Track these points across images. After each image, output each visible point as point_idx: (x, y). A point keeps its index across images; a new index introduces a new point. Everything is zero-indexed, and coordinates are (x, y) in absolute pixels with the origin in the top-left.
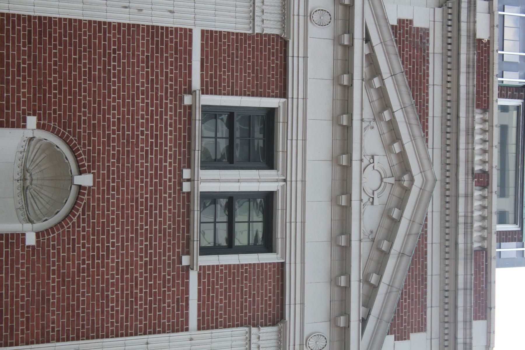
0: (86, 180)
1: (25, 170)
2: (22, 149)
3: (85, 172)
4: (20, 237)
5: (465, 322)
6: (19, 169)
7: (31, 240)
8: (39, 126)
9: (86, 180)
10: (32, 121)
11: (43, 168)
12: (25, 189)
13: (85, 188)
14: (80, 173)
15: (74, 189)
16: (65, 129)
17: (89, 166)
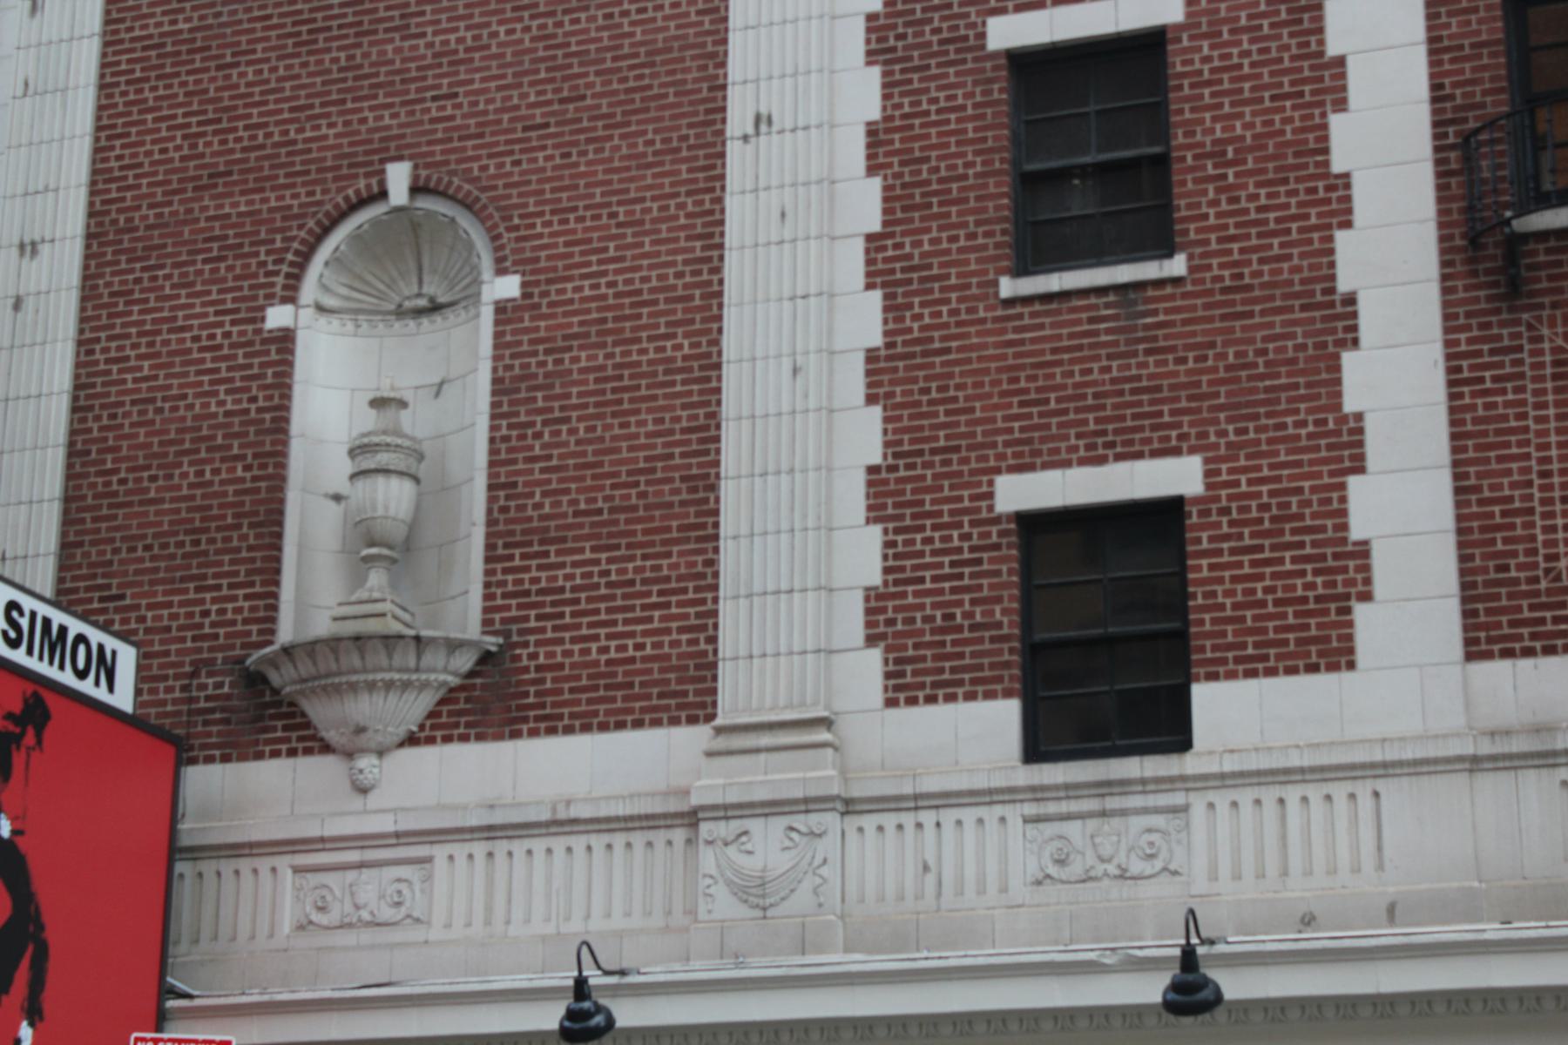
0: (398, 177)
1: (400, 313)
2: (350, 326)
3: (382, 184)
4: (501, 308)
6: (397, 325)
7: (509, 287)
8: (290, 298)
9: (398, 177)
10: (277, 317)
11: (395, 274)
12: (435, 308)
13: (415, 177)
14: (383, 194)
15: (426, 203)
16: (293, 239)
17: (367, 175)
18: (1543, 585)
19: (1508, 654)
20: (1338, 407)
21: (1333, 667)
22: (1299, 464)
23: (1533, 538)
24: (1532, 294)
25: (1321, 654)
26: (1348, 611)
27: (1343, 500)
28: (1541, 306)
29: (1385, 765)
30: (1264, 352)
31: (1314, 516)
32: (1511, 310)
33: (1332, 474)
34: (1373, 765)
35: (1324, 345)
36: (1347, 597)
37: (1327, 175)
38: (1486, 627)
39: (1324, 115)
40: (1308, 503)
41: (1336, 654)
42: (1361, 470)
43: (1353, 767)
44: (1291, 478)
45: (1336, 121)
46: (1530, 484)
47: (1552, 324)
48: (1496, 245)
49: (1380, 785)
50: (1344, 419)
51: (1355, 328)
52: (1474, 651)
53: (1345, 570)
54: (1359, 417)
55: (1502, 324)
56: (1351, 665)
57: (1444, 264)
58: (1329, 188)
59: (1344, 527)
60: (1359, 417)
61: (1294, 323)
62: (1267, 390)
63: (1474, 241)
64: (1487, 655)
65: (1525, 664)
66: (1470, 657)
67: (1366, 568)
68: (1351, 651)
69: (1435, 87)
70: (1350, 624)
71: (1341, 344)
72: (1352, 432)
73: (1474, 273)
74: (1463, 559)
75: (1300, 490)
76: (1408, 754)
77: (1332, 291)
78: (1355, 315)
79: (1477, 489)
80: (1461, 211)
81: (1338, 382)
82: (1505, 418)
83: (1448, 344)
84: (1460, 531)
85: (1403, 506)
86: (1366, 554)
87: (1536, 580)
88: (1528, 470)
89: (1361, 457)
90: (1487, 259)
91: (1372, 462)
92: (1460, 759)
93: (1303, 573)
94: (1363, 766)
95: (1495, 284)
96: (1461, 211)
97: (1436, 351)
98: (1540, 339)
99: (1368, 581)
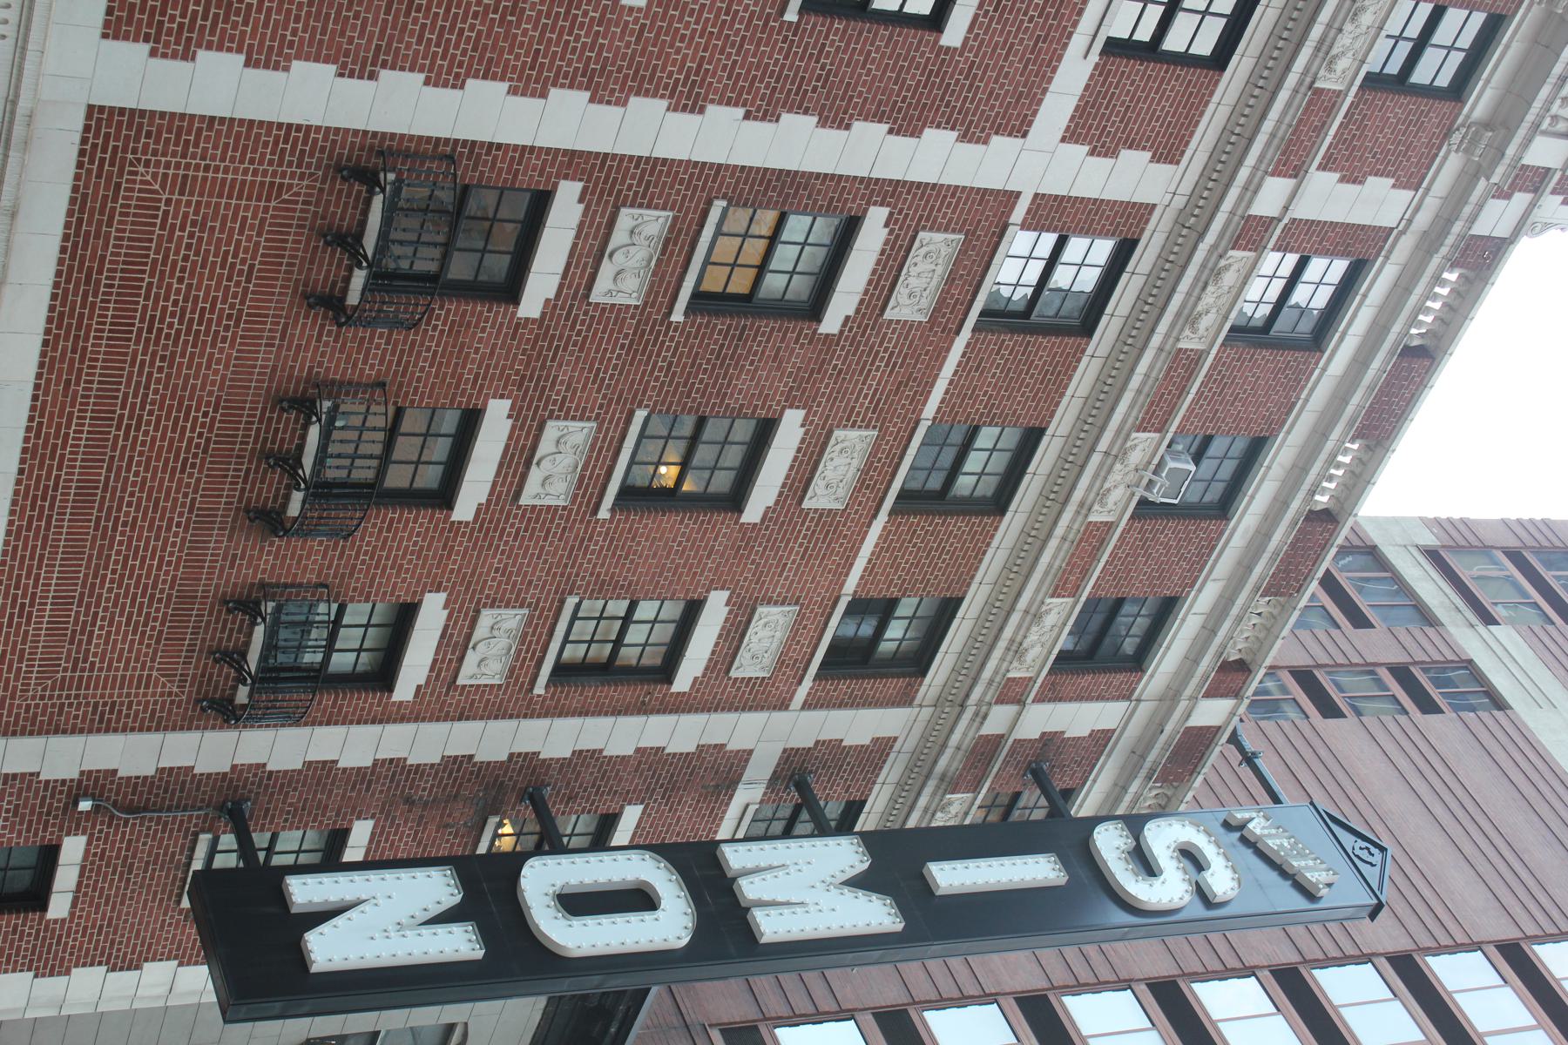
18: (130, 156)
19: (87, 128)
20: (298, 57)
21: (107, 24)
22: (266, 26)
23: (164, 154)
24: (334, 179)
25: (119, 18)
26: (146, 40)
27: (230, 50)
28: (324, 182)
29: (24, 49)
30: (356, 17)
31: (224, 30)
32: (328, 167)
33: (251, 46)
34: (26, 41)
35: (346, 55)
36: (157, 41)
37: (467, 75)
38: (110, 120)
39: (511, 80)
40: (235, 27)
41: (114, 28)
42: (247, 64)
43: (28, 29)
44: (257, 20)
45: (505, 86)
46: (203, 158)
47: (308, 187)
48: (376, 164)
49: (10, 42)
50: (288, 59)
51: (351, 75)
52: (91, 108)
53: (177, 43)
54: (286, 69)
55: (320, 160)
56: (105, 36)
57: (375, 134)
58: (457, 75)
59: (209, 47)
60: (286, 69)
61: (370, 40)
62: (328, 15)
63: (381, 153)
64: (89, 116)
65: (77, 138)
66: (91, 108)
67: (174, 56)
68: (116, 38)
69: (499, 146)
70: (136, 40)
71: (344, 66)
72: (277, 63)
73: (362, 149)
74: (163, 115)
75: (246, 23)
76: (29, 67)
77: (384, 66)
78: (361, 77)
79: (210, 128)
80: (408, 148)
81: (317, 60)
82: (254, 151)
83: (318, 129)
84: (183, 116)
85: (216, 84)
86: (185, 58)
87: (134, 151)
88: (213, 158)
89: (257, 65)
90: (365, 162)
91: (251, 71)
92: (17, 95)
93: (183, 16)
94: (26, 35)
95: (349, 159)
96: (408, 148)
97: (315, 122)
98: (302, 178)
99: (164, 56)
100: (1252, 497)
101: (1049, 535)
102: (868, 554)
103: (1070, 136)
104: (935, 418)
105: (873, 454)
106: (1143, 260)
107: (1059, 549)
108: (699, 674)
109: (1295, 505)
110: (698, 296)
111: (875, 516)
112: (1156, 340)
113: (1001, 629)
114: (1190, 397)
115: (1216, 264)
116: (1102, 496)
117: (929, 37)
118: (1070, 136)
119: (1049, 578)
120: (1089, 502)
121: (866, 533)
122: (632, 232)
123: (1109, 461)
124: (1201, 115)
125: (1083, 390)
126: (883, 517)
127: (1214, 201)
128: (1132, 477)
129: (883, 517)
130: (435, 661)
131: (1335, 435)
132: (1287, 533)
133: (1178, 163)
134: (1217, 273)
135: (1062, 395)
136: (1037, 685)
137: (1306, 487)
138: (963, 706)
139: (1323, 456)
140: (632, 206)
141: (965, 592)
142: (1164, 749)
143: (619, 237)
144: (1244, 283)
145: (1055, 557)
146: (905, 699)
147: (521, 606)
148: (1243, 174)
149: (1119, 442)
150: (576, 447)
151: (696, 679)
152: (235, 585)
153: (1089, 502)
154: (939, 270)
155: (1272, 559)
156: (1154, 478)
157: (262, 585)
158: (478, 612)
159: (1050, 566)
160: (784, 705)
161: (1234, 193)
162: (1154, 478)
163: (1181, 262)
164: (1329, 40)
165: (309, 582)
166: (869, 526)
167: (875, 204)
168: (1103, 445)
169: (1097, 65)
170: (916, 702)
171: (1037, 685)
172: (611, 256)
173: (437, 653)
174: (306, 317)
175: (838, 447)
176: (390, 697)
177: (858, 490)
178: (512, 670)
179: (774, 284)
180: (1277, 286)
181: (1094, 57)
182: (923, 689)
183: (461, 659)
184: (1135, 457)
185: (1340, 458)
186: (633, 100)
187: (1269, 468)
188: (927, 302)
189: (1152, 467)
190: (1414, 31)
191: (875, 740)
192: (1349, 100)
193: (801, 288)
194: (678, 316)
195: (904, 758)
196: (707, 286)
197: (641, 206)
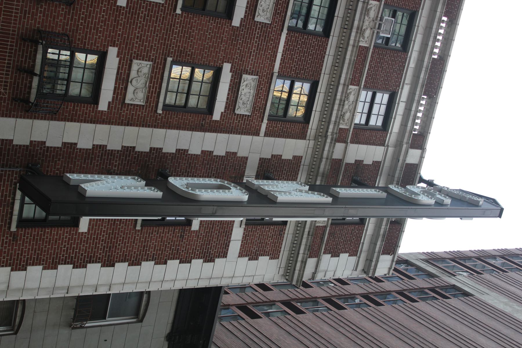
5: (344, 85)
100: (414, 41)
101: (339, 83)
102: (282, 51)
103: (241, 255)
104: (279, 72)
105: (259, 86)
106: (322, 88)
107: (352, 51)
108: (223, 111)
109: (426, 60)
110: (165, 106)
111: (282, 30)
112: (351, 42)
113: (336, 95)
114: (367, 68)
115: (346, 93)
116: (343, 116)
117: (187, 228)
118: (241, 255)
119: (351, 66)
120: (343, 99)
121: (280, 39)
122: (138, 71)
123: (346, 87)
124: (327, 45)
125: (328, 71)
126: (285, 31)
127: (338, 74)
128: (372, 24)
129: (265, 121)
130: (115, 88)
131: (418, 93)
132: (425, 74)
133: (278, 258)
134: (347, 97)
135: (320, 75)
136: (351, 132)
137: (433, 35)
138: (326, 137)
139: (436, 20)
140: (137, 59)
141: (319, 78)
142: (401, 170)
143: (133, 74)
144: (353, 115)
145: (351, 56)
146: (302, 136)
147: (149, 61)
148: (300, 258)
149: (336, 127)
150: (145, 74)
151: (222, 113)
152: (27, 28)
153: (343, 99)
154: (252, 91)
155: (426, 71)
156: (380, 22)
157: (39, 31)
158: (131, 61)
159: (350, 60)
160: (257, 134)
161: (336, 107)
162: (380, 22)
163: (345, 47)
164: (332, 148)
165: (59, 33)
166: (281, 36)
167: (226, 62)
168: (338, 97)
169: (287, 34)
170: (307, 138)
171: (351, 132)
172: (131, 82)
173: (116, 84)
174: (24, 46)
175: (245, 83)
176: (97, 107)
177: (275, 14)
178: (148, 98)
179: (193, 101)
180: (367, 105)
181: (243, 226)
182: (309, 130)
183: (126, 88)
184: (372, 14)
185: (415, 127)
186: (89, 265)
187: (418, 26)
188: (249, 106)
189: (379, 19)
190: (366, 110)
191: (294, 157)
192: (371, 50)
193: (203, 104)
194: (178, 11)
195: (306, 168)
196: (167, 102)
197: (140, 59)
